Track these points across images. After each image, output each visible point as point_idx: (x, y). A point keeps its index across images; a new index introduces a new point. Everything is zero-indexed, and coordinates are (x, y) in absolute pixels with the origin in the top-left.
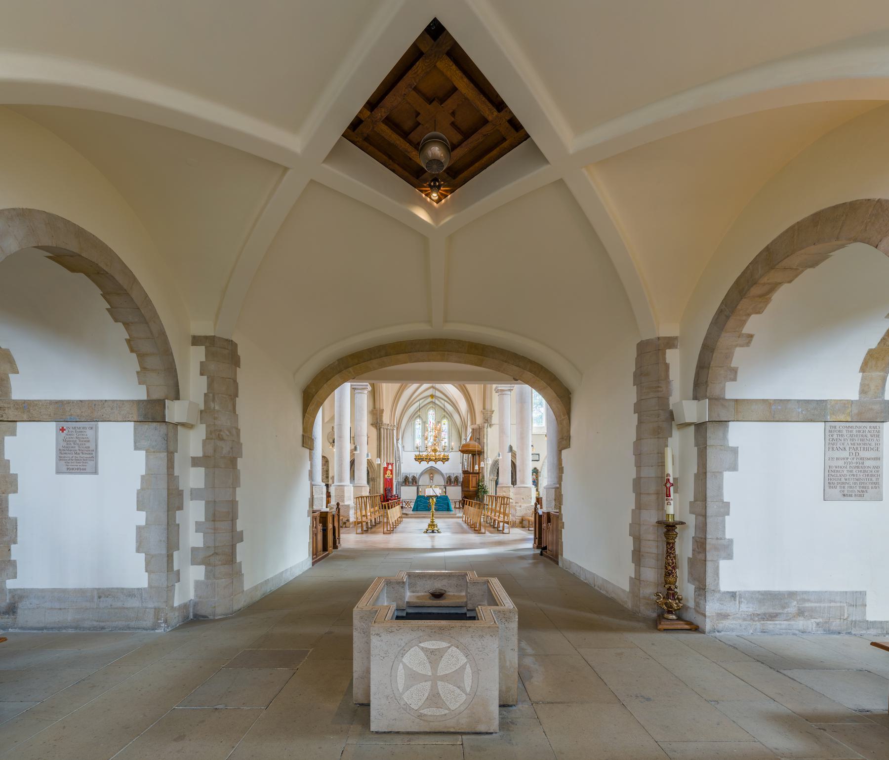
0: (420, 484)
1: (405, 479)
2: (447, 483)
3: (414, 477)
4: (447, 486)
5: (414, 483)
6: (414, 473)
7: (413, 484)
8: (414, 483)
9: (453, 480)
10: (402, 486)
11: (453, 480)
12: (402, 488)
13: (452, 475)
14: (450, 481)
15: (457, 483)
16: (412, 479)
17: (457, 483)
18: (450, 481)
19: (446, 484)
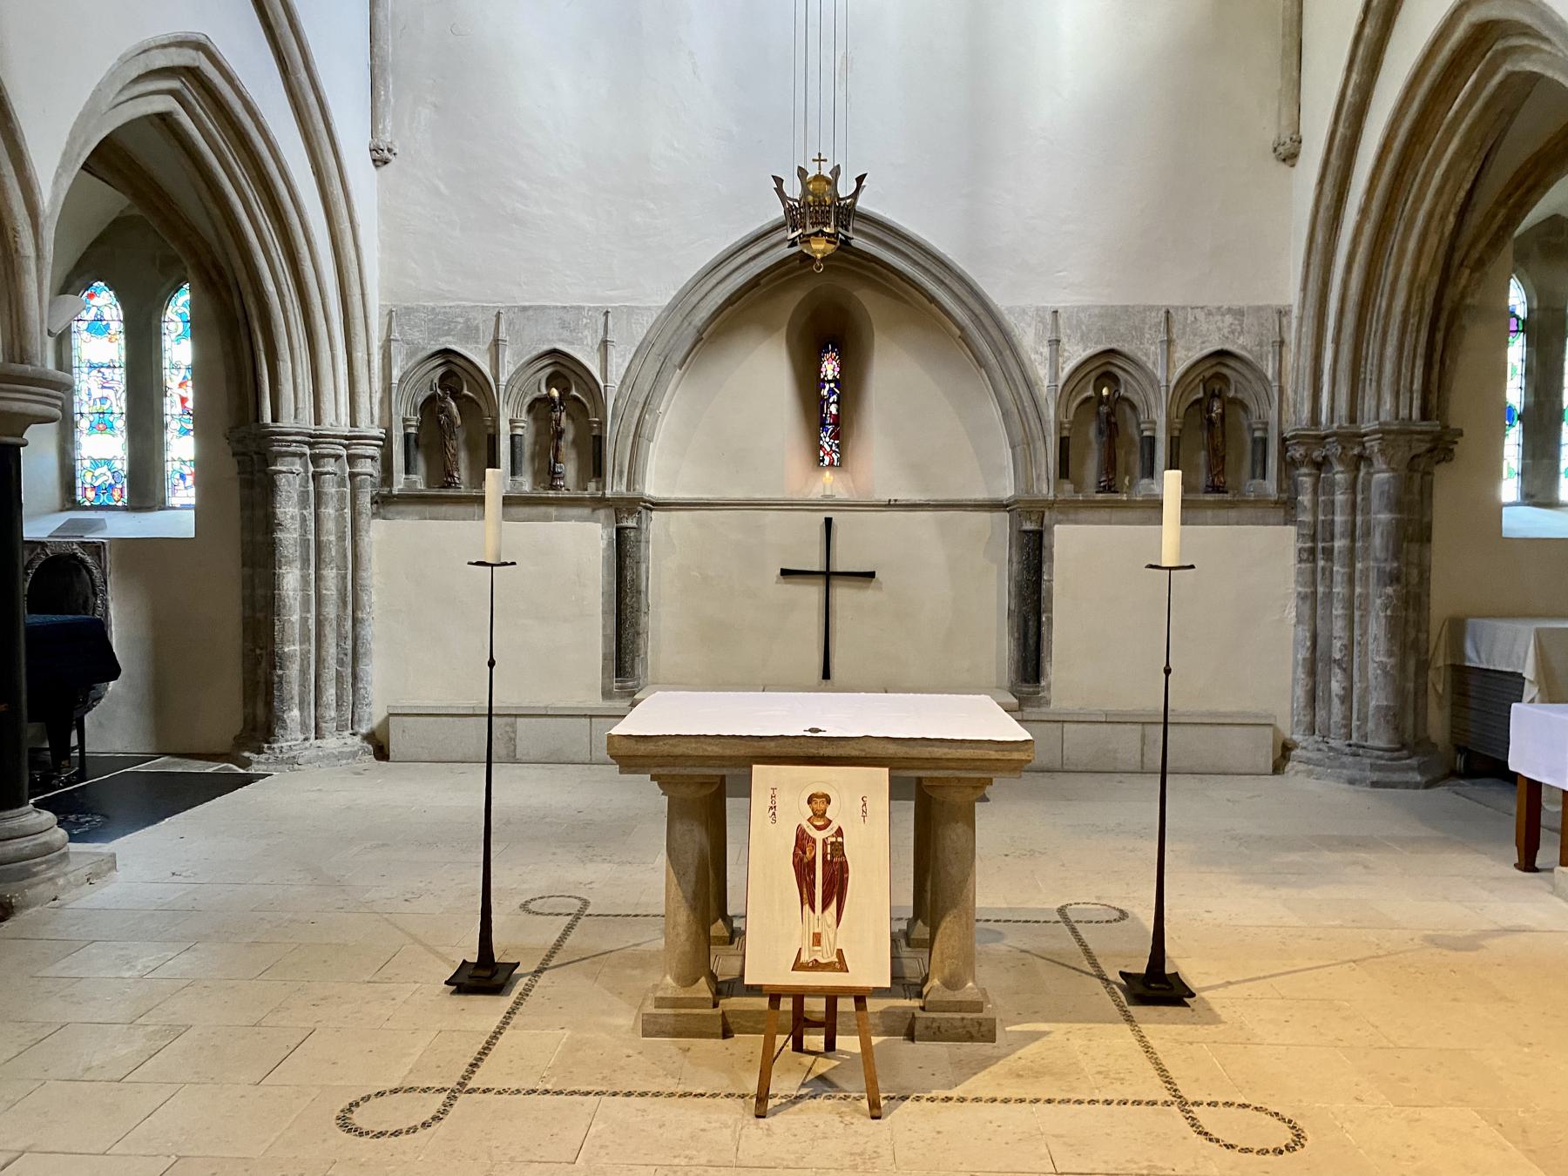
0: (652, 488)
1: (430, 407)
2: (1064, 471)
3: (562, 368)
4: (1071, 509)
5: (569, 468)
6: (570, 316)
7: (548, 475)
8: (569, 468)
9: (1158, 418)
10: (385, 502)
11: (1158, 418)
12: (377, 532)
13: (1148, 351)
14: (1111, 430)
15: (1217, 461)
16: (540, 408)
17: (1217, 461)
18: (1111, 430)
19: (1045, 490)
